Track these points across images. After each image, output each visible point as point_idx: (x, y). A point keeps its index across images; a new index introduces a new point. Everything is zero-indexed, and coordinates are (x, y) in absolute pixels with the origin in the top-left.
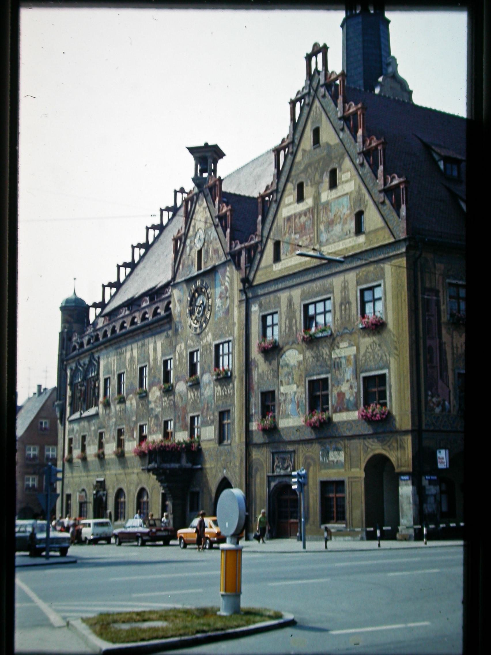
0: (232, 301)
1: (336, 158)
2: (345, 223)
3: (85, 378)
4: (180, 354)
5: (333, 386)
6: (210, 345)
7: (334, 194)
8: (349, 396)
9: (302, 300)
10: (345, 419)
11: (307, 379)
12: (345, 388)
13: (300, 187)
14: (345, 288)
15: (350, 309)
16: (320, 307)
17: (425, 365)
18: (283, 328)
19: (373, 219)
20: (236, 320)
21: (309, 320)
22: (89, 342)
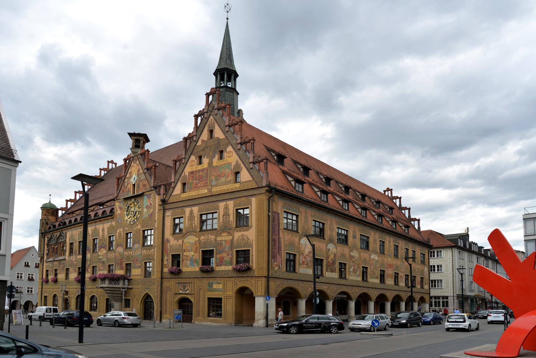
0: (154, 209)
1: (223, 145)
2: (228, 176)
3: (57, 243)
4: (120, 234)
5: (216, 254)
6: (140, 230)
7: (221, 162)
8: (227, 259)
9: (199, 212)
10: (224, 269)
11: (201, 250)
12: (224, 255)
13: (200, 157)
14: (226, 208)
15: (229, 218)
16: (210, 216)
17: (272, 247)
18: (187, 225)
19: (245, 176)
20: (156, 219)
21: (202, 222)
22: (59, 225)
